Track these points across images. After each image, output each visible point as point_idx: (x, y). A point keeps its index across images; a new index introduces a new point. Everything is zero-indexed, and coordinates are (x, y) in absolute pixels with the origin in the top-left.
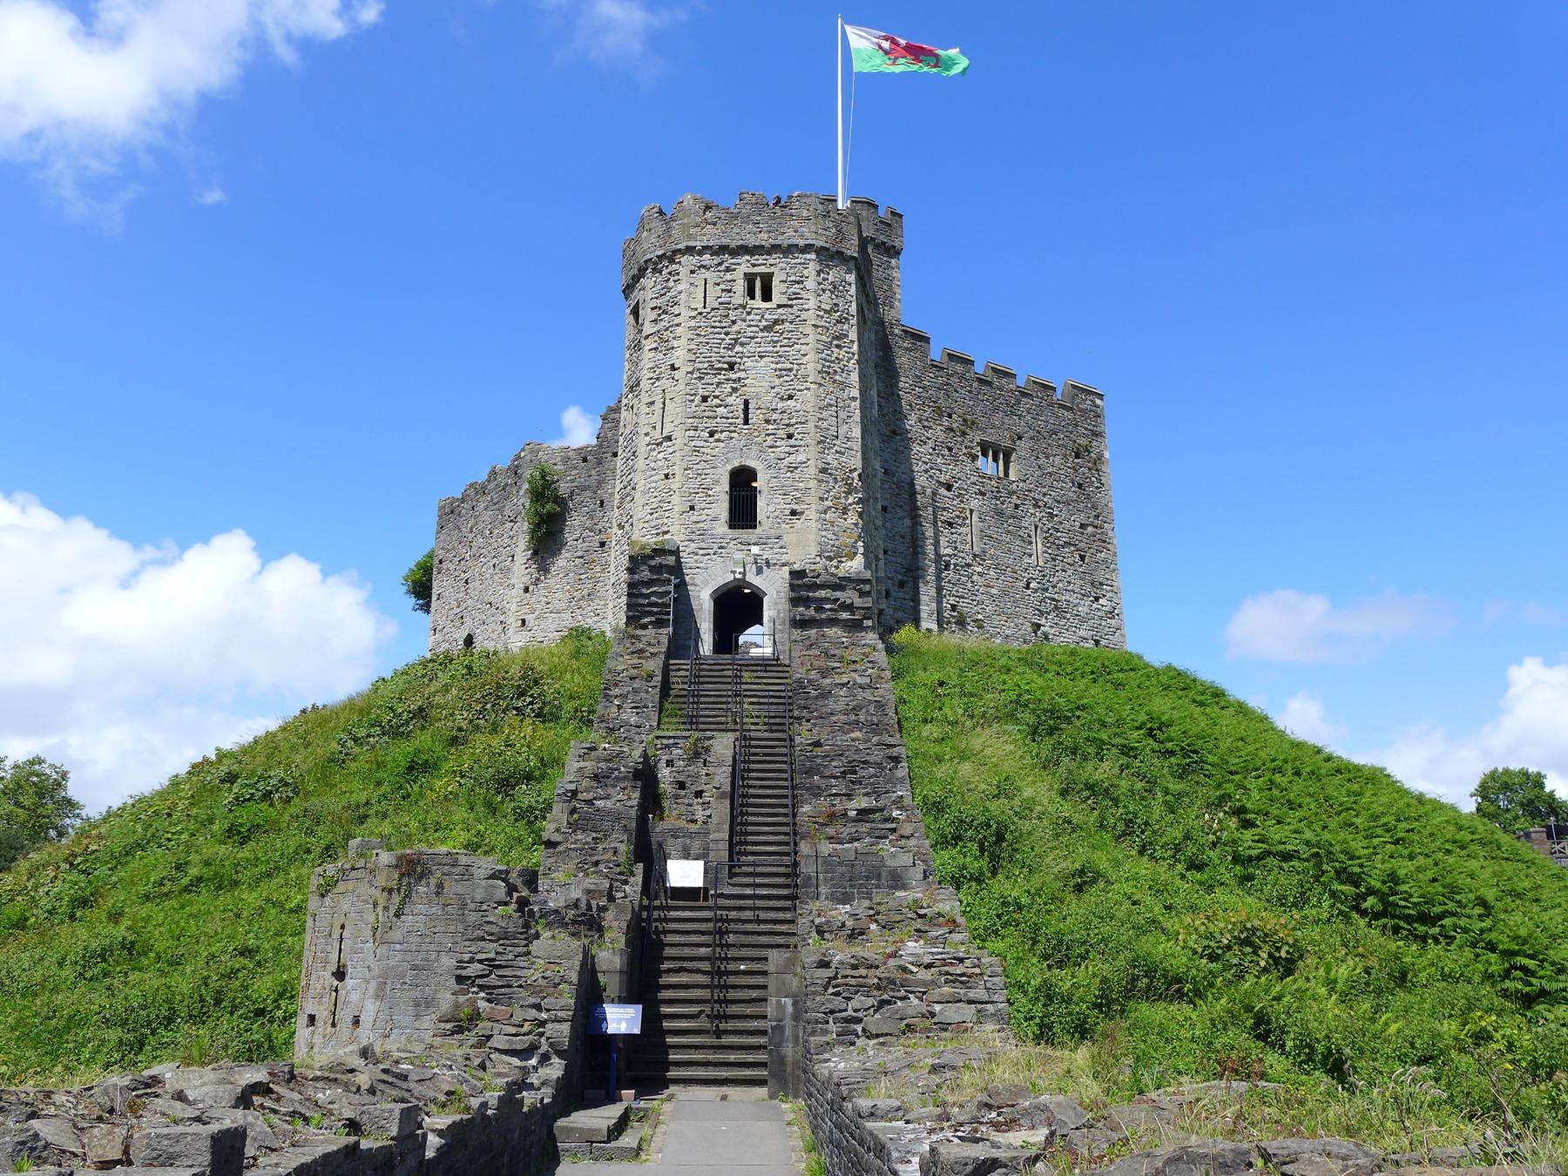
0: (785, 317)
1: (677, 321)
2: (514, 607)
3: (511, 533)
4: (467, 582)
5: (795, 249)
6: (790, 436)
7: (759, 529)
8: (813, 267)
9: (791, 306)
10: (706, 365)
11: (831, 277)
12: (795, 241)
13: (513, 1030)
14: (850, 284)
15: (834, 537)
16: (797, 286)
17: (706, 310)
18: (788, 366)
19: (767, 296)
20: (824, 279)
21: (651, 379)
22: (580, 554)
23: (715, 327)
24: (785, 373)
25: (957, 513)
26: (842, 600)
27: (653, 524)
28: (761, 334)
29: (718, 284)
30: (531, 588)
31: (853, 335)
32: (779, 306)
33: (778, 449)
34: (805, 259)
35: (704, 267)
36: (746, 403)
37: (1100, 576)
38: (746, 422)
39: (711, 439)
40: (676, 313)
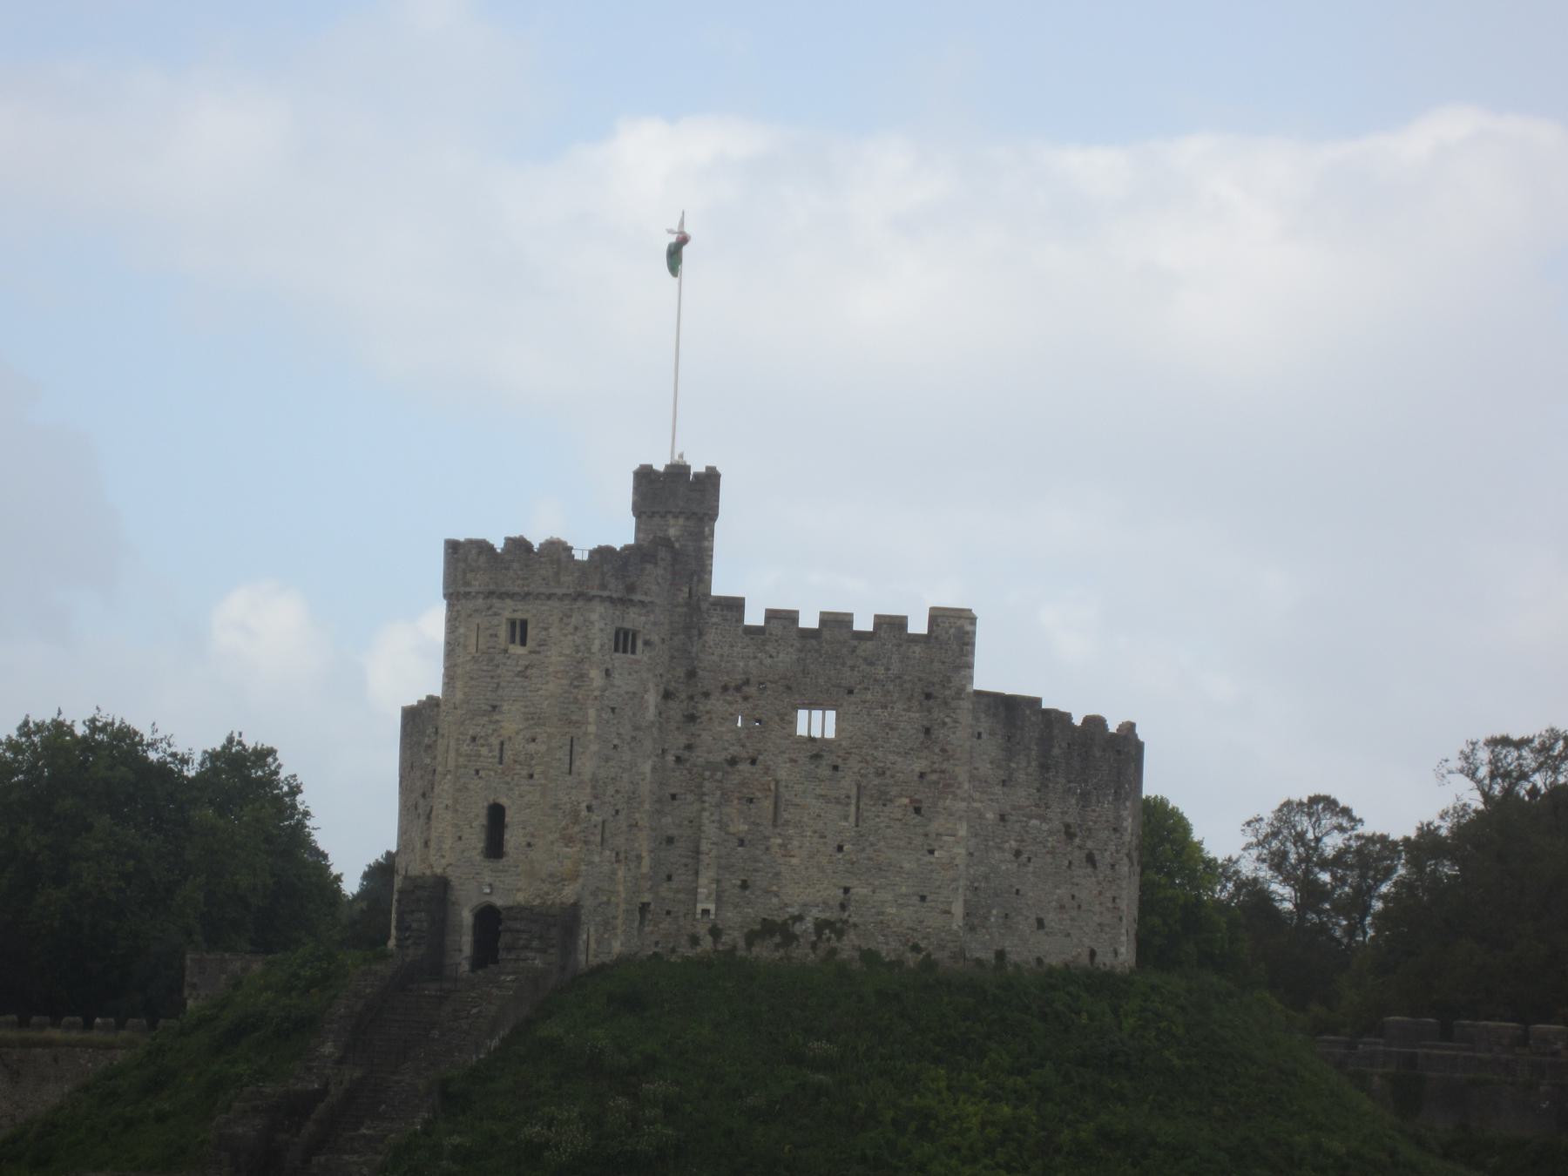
5: (543, 597)
6: (531, 776)
7: (504, 859)
11: (573, 621)
14: (592, 623)
16: (544, 633)
18: (532, 709)
19: (523, 643)
20: (567, 624)
23: (483, 671)
24: (530, 716)
31: (596, 675)
32: (531, 652)
35: (476, 611)
36: (502, 744)
38: (501, 762)
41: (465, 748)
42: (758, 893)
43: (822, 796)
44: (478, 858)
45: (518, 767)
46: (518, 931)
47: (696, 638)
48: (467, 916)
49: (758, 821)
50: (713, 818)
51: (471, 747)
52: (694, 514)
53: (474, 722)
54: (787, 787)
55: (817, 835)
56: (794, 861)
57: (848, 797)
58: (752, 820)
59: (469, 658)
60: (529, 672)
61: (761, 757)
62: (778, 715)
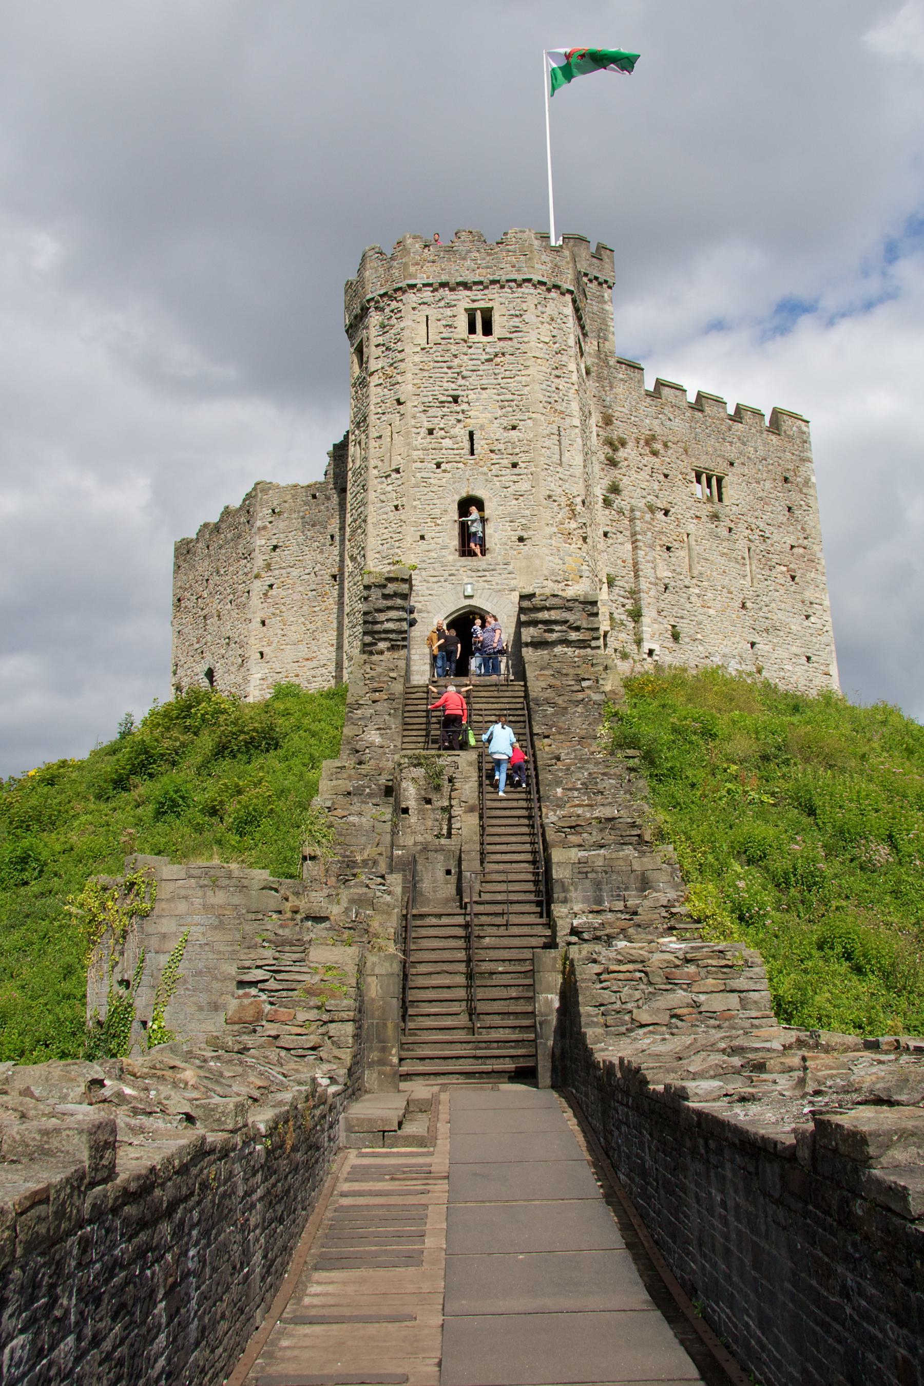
0: (505, 350)
1: (400, 356)
3: (246, 570)
4: (205, 617)
5: (512, 285)
6: (515, 465)
7: (488, 556)
8: (531, 302)
9: (511, 339)
10: (431, 399)
11: (549, 311)
13: (299, 1030)
15: (561, 562)
17: (429, 346)
18: (510, 397)
20: (543, 313)
21: (377, 414)
22: (314, 587)
24: (506, 404)
25: (675, 537)
26: (572, 621)
27: (384, 555)
28: (482, 367)
29: (439, 320)
30: (267, 622)
31: (572, 367)
33: (503, 478)
34: (523, 293)
35: (424, 303)
36: (471, 434)
37: (809, 595)
38: (472, 453)
39: (438, 471)
40: (400, 349)
41: (421, 440)
42: (687, 640)
43: (724, 554)
44: (451, 558)
45: (493, 456)
46: (545, 622)
47: (608, 388)
49: (678, 570)
50: (648, 558)
51: (428, 440)
52: (596, 278)
53: (429, 414)
54: (696, 541)
55: (725, 590)
57: (744, 558)
58: (673, 568)
59: (418, 349)
60: (498, 360)
61: (673, 510)
62: (681, 473)
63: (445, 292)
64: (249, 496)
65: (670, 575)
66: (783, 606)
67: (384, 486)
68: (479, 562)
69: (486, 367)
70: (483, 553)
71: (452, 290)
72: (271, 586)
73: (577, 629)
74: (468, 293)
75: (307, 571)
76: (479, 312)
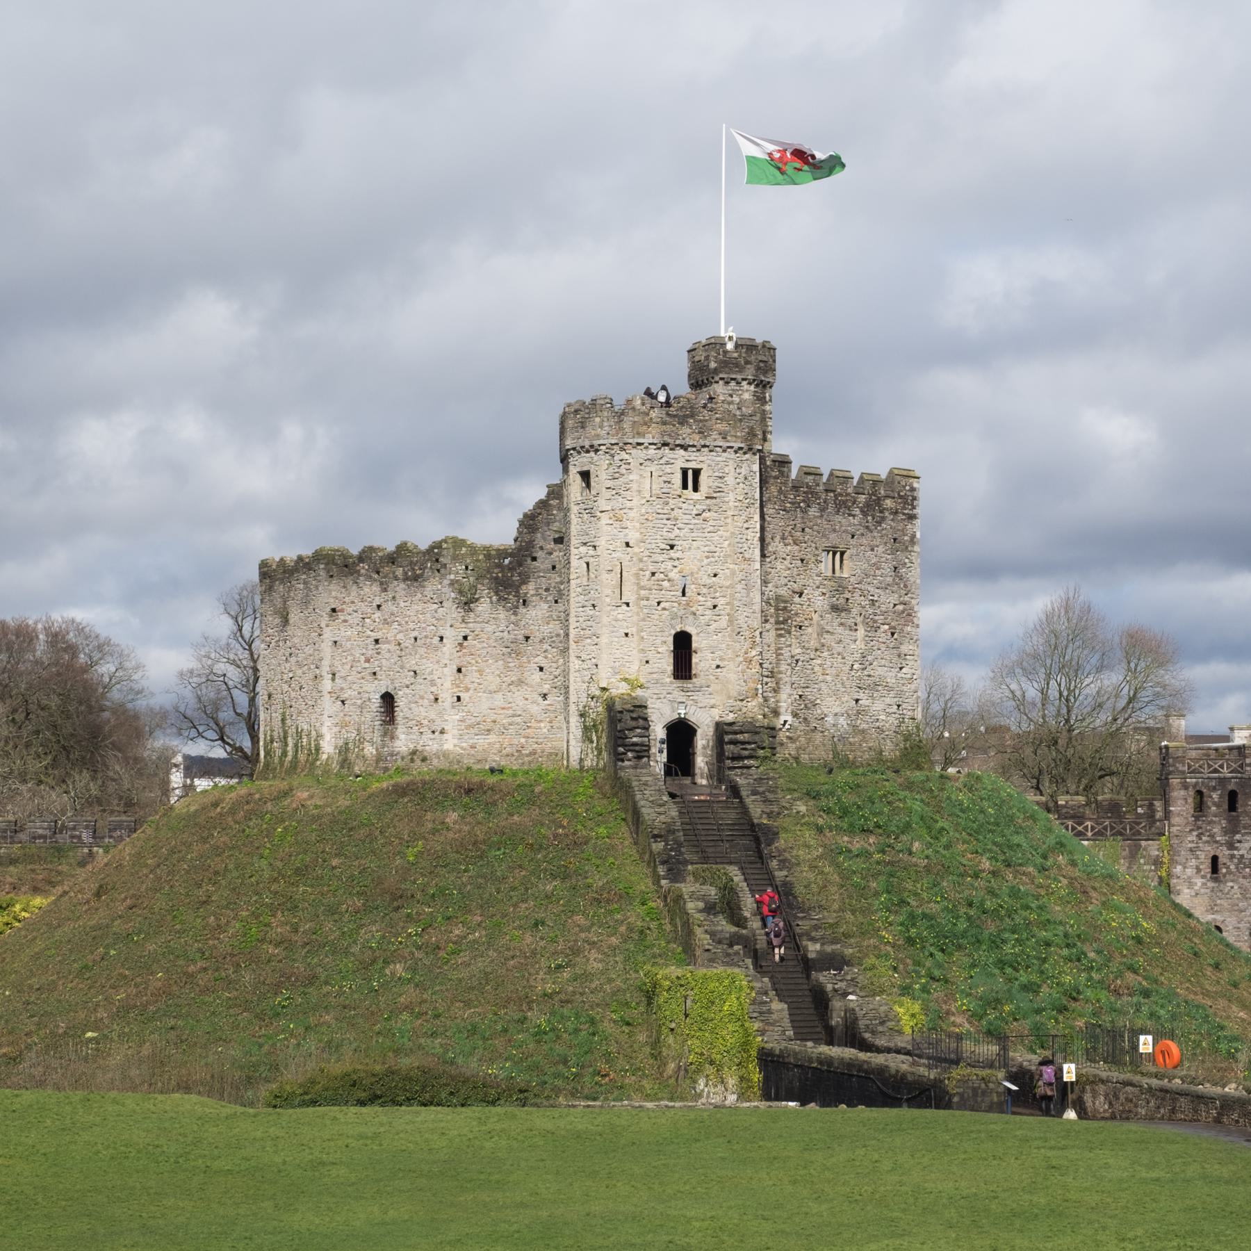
1: (629, 504)
2: (448, 684)
4: (377, 641)
5: (718, 449)
6: (715, 607)
7: (694, 680)
8: (730, 468)
12: (721, 444)
19: (696, 489)
30: (463, 669)
37: (904, 648)
44: (668, 680)
45: (700, 598)
46: (743, 743)
48: (659, 732)
56: (829, 678)
59: (644, 501)
63: (666, 450)
64: (438, 545)
65: (799, 651)
66: (883, 662)
67: (615, 613)
68: (688, 685)
69: (696, 521)
70: (690, 678)
71: (671, 449)
72: (465, 638)
73: (763, 748)
74: (682, 452)
75: (500, 629)
76: (690, 473)
